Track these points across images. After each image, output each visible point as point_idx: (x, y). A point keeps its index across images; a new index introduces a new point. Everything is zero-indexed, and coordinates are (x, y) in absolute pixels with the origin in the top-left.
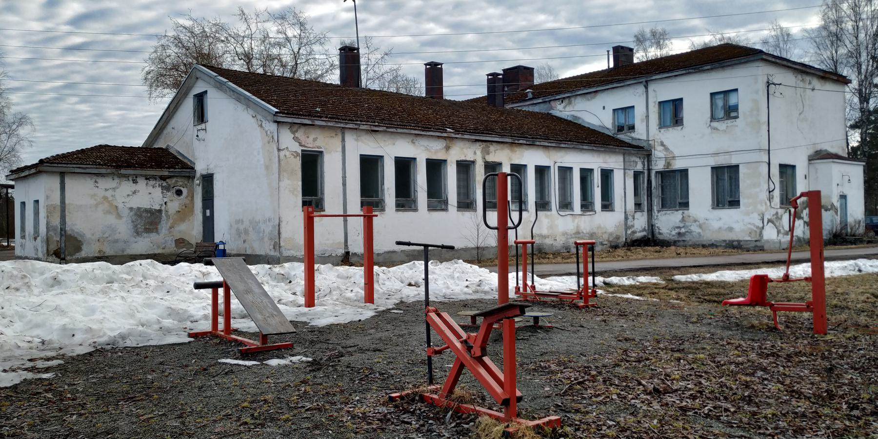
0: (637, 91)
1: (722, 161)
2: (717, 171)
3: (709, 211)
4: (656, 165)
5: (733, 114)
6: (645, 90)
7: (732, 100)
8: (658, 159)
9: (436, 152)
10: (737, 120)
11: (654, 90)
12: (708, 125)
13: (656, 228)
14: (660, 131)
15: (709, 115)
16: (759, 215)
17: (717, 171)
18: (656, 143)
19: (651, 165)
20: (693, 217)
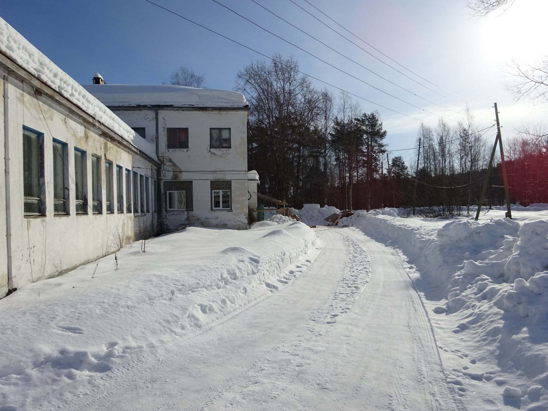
0: (147, 116)
1: (219, 176)
2: (215, 185)
3: (209, 212)
4: (164, 176)
5: (225, 145)
6: (155, 117)
7: (225, 135)
8: (166, 172)
9: (80, 140)
10: (230, 149)
11: (163, 119)
12: (208, 151)
13: (165, 225)
14: (168, 151)
15: (209, 144)
16: (245, 215)
17: (215, 185)
18: (165, 160)
19: (161, 177)
20: (196, 217)
